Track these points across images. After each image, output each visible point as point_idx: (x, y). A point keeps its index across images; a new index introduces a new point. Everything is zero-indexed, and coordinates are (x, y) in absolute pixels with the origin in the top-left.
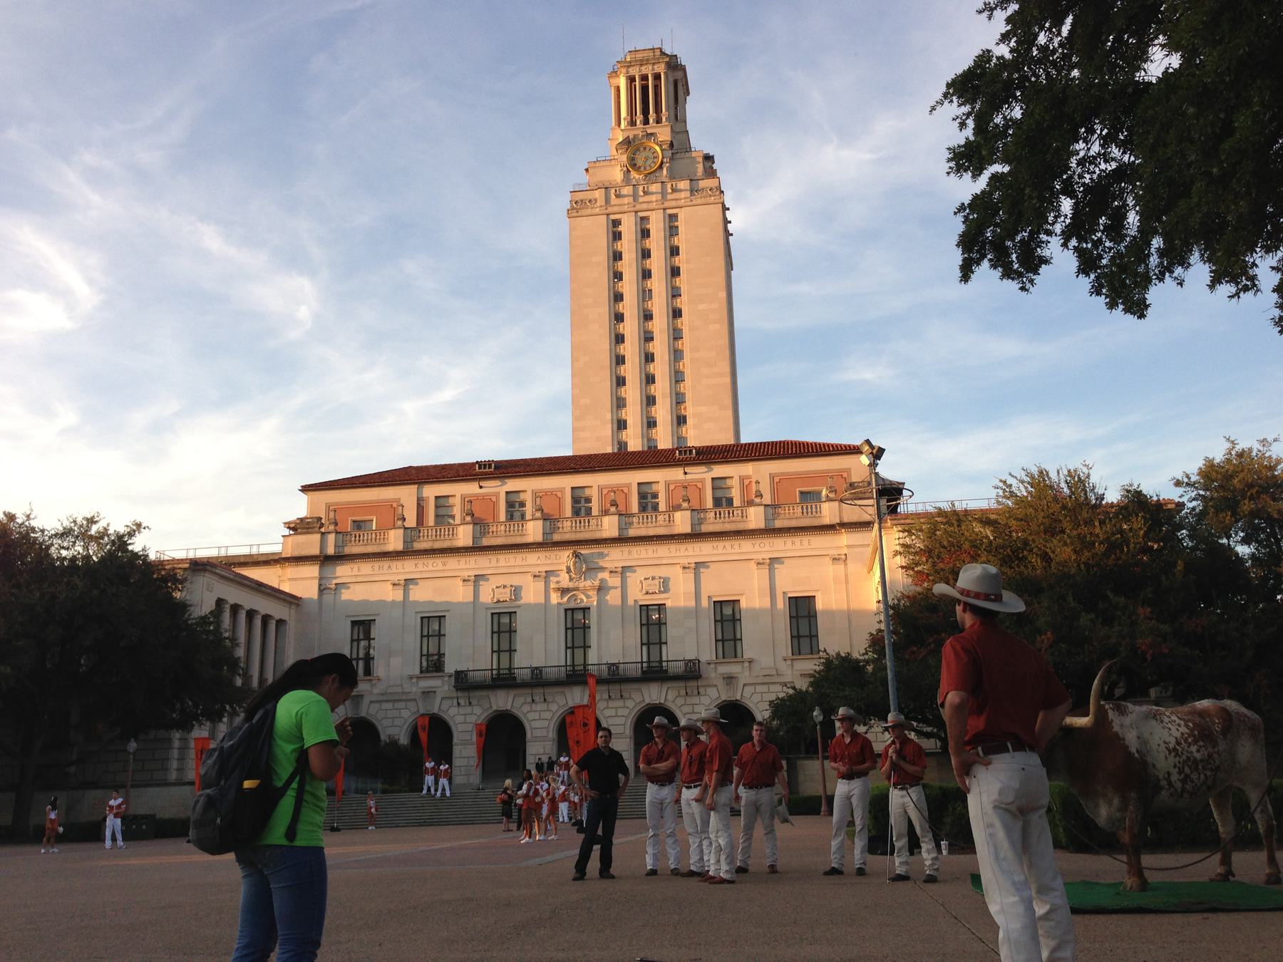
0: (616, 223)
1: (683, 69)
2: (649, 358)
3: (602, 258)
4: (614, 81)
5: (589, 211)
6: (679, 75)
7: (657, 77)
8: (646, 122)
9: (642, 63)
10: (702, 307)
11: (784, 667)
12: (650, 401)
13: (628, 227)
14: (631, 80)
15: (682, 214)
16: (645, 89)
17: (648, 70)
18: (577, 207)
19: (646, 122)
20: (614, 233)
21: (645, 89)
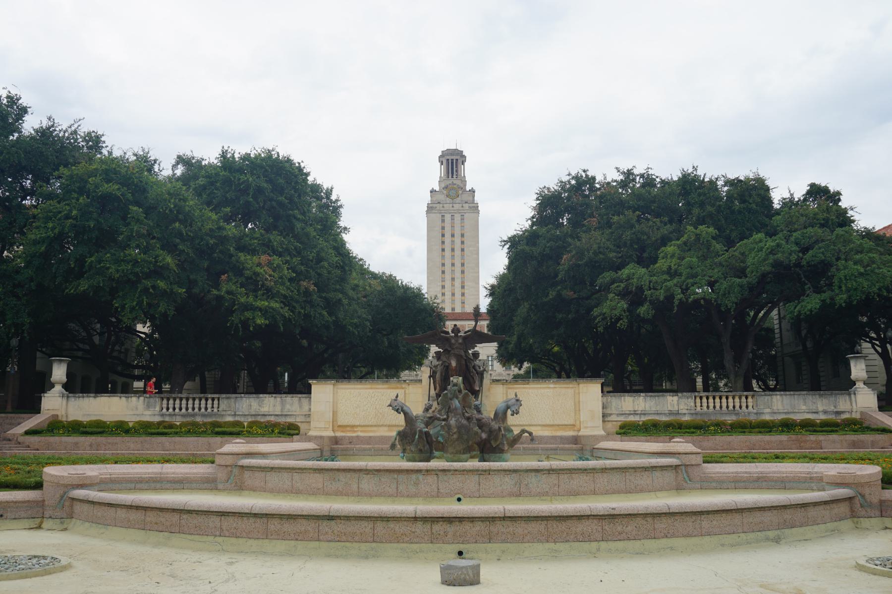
0: (443, 216)
1: (465, 157)
2: (453, 265)
3: (439, 229)
4: (441, 159)
5: (434, 211)
6: (464, 159)
7: (457, 160)
8: (452, 177)
9: (452, 154)
10: (471, 249)
11: (503, 372)
12: (453, 279)
13: (448, 217)
14: (448, 160)
15: (466, 216)
16: (452, 163)
17: (454, 157)
18: (430, 209)
19: (452, 177)
20: (442, 220)
21: (452, 163)
